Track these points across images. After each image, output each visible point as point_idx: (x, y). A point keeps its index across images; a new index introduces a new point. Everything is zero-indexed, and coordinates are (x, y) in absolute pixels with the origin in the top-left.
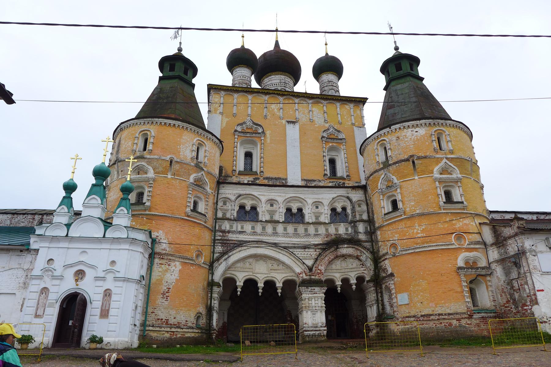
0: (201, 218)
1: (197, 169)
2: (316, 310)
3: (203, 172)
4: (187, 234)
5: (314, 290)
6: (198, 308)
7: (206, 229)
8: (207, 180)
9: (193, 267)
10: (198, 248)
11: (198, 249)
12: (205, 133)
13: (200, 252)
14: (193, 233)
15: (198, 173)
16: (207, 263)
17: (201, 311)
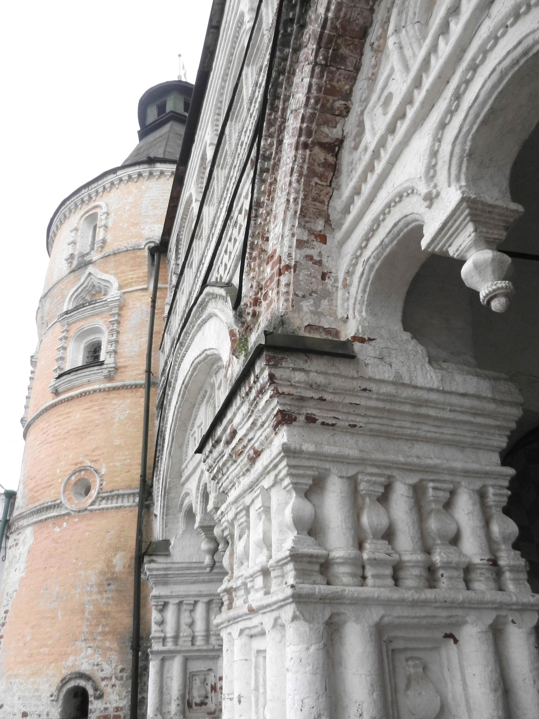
0: (86, 379)
1: (77, 273)
2: (252, 611)
3: (90, 269)
4: (50, 443)
5: (234, 433)
6: (71, 658)
7: (113, 395)
8: (105, 276)
9: (60, 526)
10: (76, 464)
11: (79, 465)
12: (96, 184)
13: (85, 469)
14: (64, 431)
15: (79, 279)
16: (121, 492)
17: (85, 668)
